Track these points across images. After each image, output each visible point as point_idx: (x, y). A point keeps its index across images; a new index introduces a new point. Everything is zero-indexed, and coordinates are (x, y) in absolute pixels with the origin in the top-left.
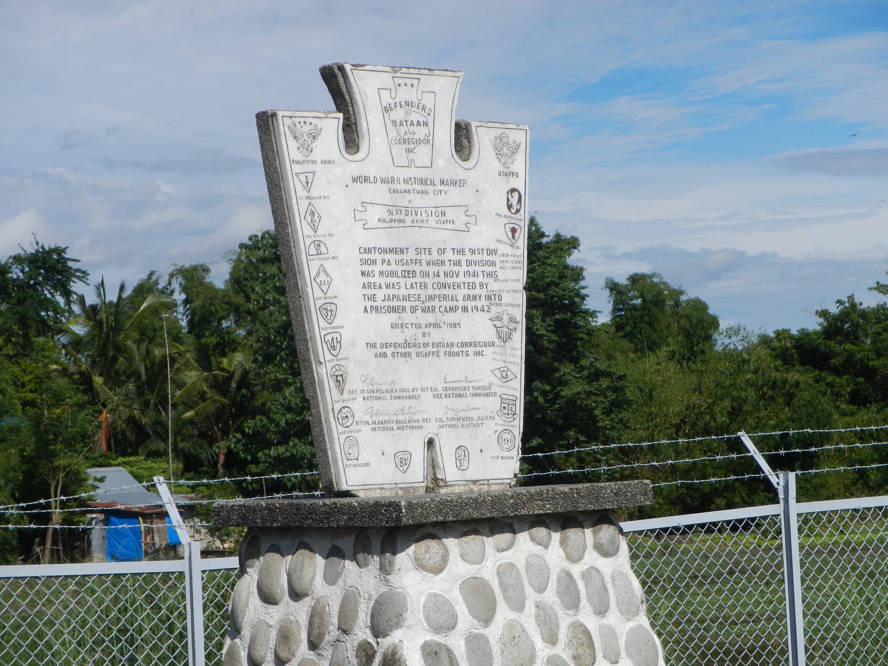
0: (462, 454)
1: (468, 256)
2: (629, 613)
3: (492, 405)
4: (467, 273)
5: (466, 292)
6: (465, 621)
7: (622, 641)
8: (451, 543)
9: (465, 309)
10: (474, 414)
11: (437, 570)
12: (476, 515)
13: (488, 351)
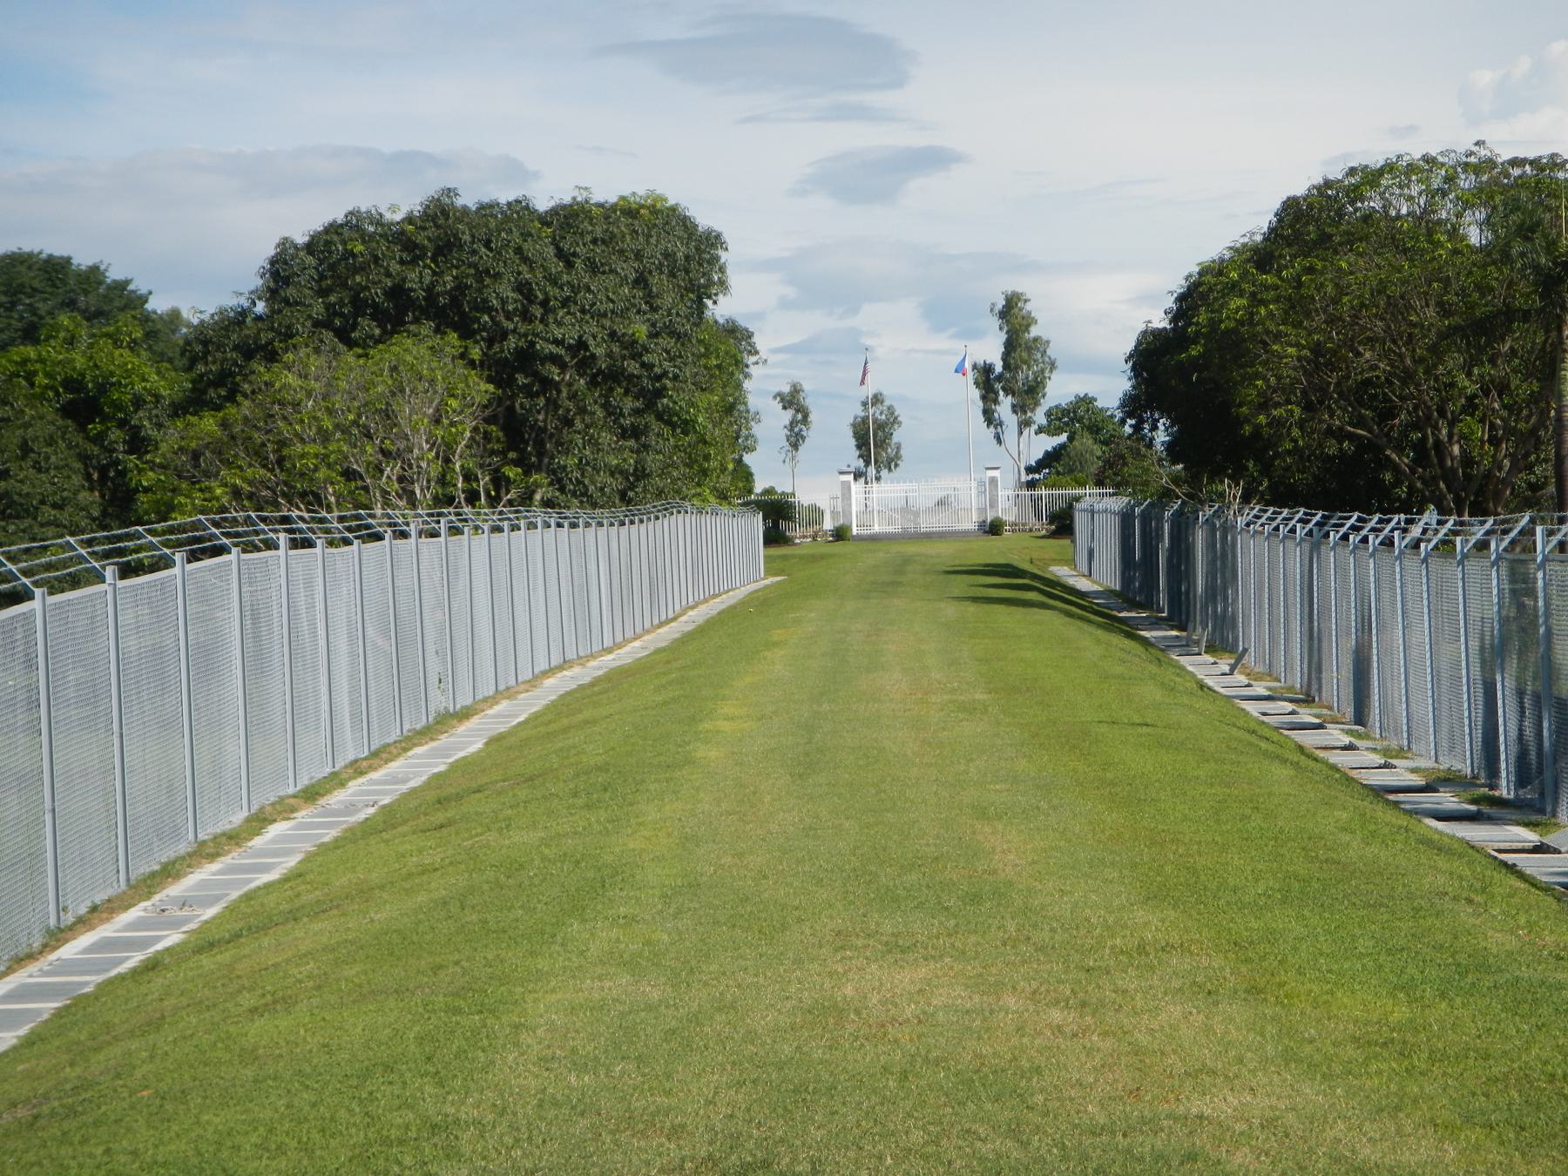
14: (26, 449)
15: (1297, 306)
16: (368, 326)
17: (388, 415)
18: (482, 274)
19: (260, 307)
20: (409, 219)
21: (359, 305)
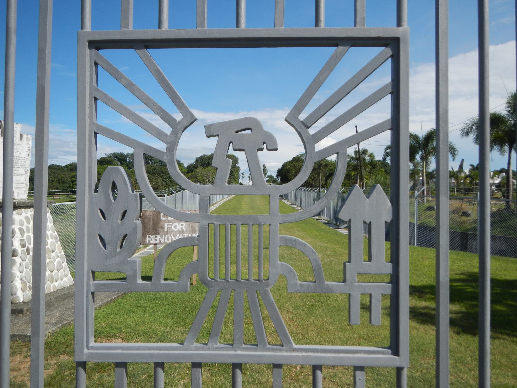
0: (18, 193)
1: (21, 158)
2: (51, 223)
3: (23, 185)
4: (21, 161)
5: (20, 165)
6: (26, 224)
7: (50, 227)
8: (23, 210)
9: (20, 168)
10: (20, 187)
11: (21, 215)
12: (28, 205)
13: (23, 175)
15: (294, 167)
16: (205, 166)
17: (207, 174)
19: (195, 163)
20: (209, 155)
21: (204, 164)
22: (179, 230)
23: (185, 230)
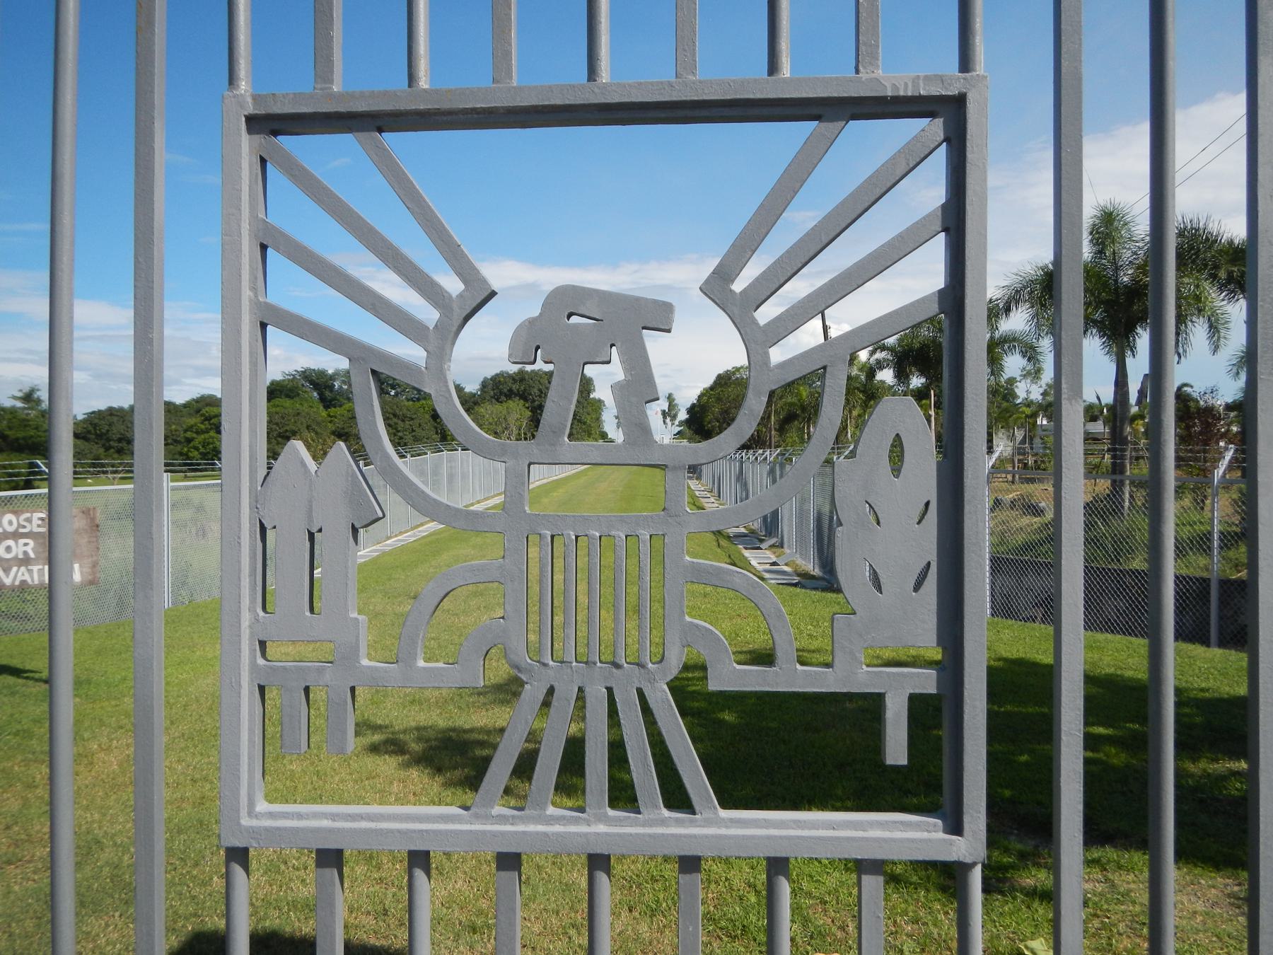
14: (420, 425)
15: (719, 399)
16: (503, 398)
17: (505, 419)
18: (529, 387)
20: (514, 373)
21: (501, 393)
22: (16, 558)
23: (32, 555)
